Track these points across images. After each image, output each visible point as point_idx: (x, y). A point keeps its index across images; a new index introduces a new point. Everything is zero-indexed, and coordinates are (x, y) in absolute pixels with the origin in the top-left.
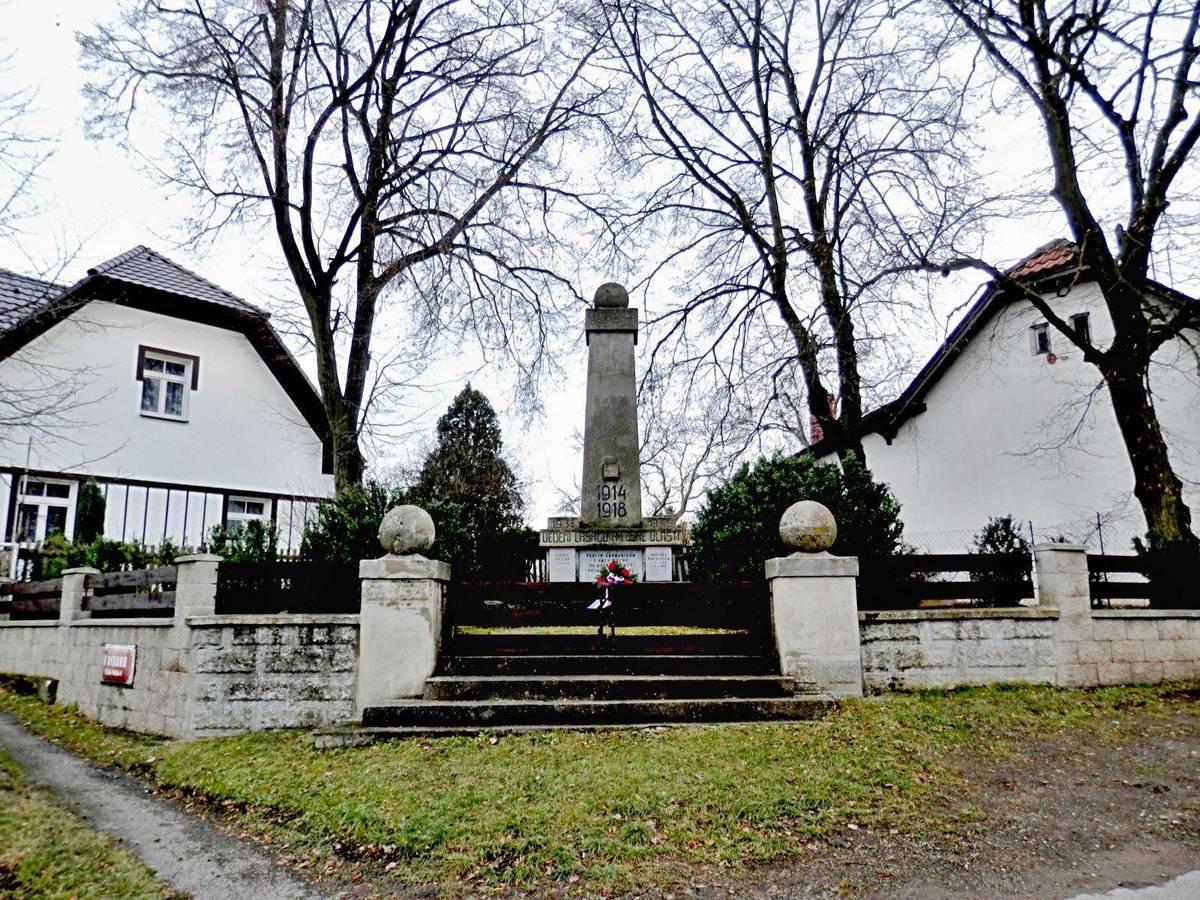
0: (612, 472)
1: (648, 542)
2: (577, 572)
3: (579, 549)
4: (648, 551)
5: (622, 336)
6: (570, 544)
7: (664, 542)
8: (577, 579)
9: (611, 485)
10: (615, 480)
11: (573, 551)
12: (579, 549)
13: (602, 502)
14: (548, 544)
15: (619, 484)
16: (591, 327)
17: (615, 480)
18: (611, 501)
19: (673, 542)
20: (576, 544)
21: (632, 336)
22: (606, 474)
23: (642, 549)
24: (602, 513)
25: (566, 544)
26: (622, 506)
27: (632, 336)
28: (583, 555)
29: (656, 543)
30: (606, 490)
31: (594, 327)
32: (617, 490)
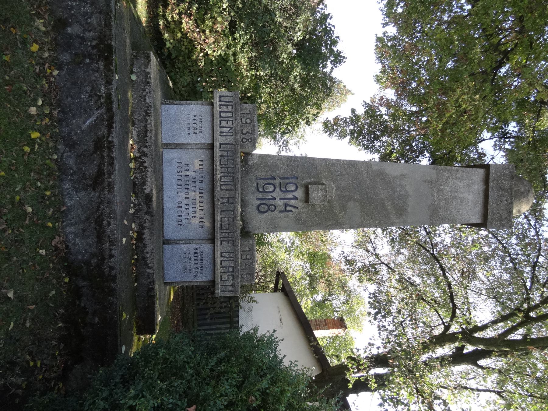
0: (316, 194)
1: (219, 249)
3: (211, 147)
4: (206, 248)
5: (479, 208)
6: (217, 134)
7: (219, 270)
8: (168, 146)
9: (300, 193)
10: (307, 200)
11: (209, 141)
12: (211, 147)
13: (277, 182)
16: (492, 171)
17: (307, 200)
18: (277, 194)
19: (219, 284)
20: (217, 144)
21: (476, 219)
22: (312, 188)
23: (212, 240)
24: (262, 183)
26: (271, 208)
27: (476, 219)
28: (203, 155)
29: (218, 260)
31: (492, 176)
32: (292, 202)
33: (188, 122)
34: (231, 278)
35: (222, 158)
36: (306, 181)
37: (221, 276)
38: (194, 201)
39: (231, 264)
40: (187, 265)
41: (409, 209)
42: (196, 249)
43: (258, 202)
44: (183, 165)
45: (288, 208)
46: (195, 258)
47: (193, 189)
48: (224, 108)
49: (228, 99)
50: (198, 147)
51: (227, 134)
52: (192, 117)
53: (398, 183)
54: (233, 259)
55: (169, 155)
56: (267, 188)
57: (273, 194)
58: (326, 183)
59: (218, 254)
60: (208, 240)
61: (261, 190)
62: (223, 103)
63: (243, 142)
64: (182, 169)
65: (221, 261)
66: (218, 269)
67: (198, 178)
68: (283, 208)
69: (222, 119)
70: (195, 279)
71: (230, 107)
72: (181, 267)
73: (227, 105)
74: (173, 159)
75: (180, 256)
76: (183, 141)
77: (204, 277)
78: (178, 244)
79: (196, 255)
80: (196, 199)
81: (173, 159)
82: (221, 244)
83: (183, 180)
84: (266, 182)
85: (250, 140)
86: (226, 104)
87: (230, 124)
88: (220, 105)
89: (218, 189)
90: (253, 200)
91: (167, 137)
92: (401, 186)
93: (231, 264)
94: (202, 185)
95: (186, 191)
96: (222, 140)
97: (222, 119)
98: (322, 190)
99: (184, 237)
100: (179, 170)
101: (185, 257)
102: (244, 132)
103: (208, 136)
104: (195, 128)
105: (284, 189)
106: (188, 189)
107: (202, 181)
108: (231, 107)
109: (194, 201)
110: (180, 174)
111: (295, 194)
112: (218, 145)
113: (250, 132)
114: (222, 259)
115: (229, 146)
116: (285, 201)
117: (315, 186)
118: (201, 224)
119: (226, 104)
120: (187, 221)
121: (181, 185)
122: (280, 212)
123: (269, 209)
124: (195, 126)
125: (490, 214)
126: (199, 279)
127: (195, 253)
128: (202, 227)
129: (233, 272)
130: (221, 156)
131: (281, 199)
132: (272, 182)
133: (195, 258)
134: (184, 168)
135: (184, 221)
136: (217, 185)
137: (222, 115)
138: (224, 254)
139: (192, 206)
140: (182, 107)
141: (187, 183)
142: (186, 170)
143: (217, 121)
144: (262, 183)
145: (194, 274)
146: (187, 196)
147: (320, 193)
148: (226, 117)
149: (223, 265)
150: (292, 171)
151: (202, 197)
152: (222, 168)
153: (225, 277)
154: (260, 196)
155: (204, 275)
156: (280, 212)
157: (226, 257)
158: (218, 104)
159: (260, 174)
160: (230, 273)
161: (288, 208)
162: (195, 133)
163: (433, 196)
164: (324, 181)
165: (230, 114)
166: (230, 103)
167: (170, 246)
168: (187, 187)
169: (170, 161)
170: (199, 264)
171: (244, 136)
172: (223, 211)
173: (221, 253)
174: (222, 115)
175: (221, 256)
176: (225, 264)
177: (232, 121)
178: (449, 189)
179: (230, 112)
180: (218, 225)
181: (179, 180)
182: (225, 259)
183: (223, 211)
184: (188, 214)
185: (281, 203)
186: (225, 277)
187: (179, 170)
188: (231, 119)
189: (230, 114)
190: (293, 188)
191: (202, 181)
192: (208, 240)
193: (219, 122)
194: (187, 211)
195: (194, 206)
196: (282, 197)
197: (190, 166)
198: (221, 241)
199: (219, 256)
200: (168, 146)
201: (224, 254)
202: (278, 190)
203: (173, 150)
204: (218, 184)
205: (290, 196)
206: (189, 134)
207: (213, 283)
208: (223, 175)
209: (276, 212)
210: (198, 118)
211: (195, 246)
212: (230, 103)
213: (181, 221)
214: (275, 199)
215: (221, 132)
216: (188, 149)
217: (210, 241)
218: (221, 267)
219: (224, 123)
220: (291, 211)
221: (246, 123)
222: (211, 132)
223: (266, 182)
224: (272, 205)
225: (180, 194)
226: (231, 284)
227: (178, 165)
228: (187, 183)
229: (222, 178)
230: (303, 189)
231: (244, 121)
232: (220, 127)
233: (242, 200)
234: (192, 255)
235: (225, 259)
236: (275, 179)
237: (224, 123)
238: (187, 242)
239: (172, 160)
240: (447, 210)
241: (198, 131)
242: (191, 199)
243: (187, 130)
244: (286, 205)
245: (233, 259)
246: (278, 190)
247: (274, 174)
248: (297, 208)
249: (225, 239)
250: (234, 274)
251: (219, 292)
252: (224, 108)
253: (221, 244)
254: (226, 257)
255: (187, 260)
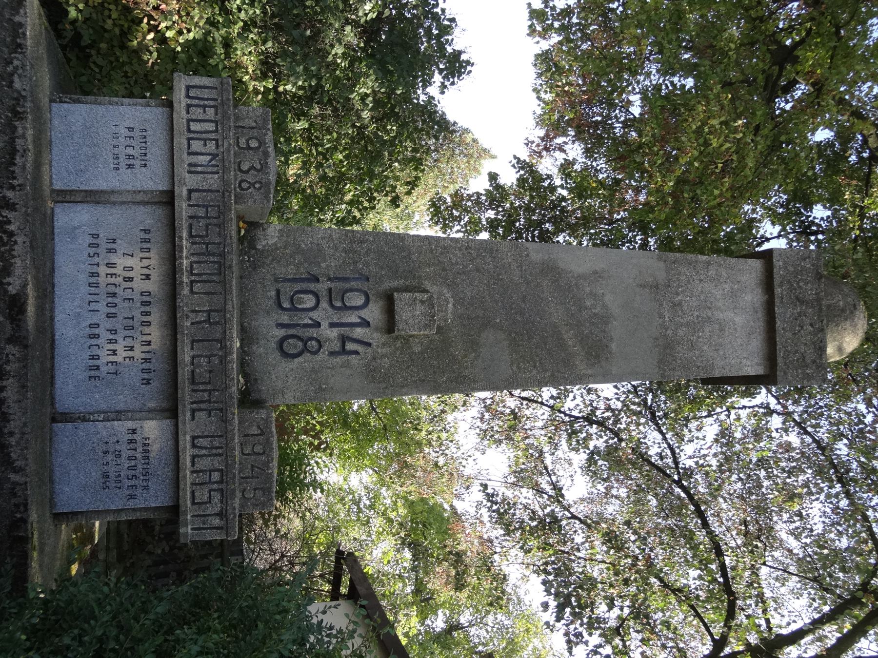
0: (410, 313)
2: (93, 197)
3: (168, 199)
5: (757, 343)
6: (181, 170)
8: (66, 196)
9: (374, 313)
10: (390, 325)
11: (162, 185)
12: (168, 199)
13: (322, 287)
14: (180, 97)
15: (376, 337)
16: (778, 263)
17: (390, 325)
19: (189, 512)
20: (182, 192)
21: (753, 367)
22: (402, 300)
23: (172, 412)
24: (288, 289)
25: (184, 160)
28: (149, 217)
30: (359, 301)
31: (779, 273)
32: (359, 332)
33: (115, 142)
34: (216, 497)
35: (194, 222)
36: (388, 285)
37: (193, 493)
38: (130, 322)
39: (217, 463)
40: (112, 470)
41: (613, 346)
42: (134, 431)
43: (282, 333)
44: (102, 241)
45: (350, 346)
46: (131, 453)
47: (128, 294)
48: (197, 113)
49: (206, 94)
50: (139, 198)
51: (205, 169)
52: (124, 132)
53: (588, 289)
54: (220, 451)
55: (70, 219)
56: (300, 301)
57: (315, 315)
58: (434, 289)
59: (186, 440)
60: (162, 410)
61: (286, 305)
62: (196, 102)
63: (242, 189)
64: (102, 250)
65: (193, 457)
66: (185, 476)
67: (137, 268)
68: (336, 346)
69: (192, 135)
70: (131, 504)
71: (211, 112)
72: (96, 475)
73: (204, 107)
74: (80, 227)
75: (94, 449)
76: (100, 185)
77: (155, 497)
78: (89, 421)
79: (132, 446)
80: (133, 318)
81: (80, 227)
82: (193, 418)
83: (102, 274)
84: (298, 287)
85: (257, 186)
86: (202, 103)
87: (211, 147)
88: (189, 106)
89: (186, 291)
90: (270, 329)
91: (65, 174)
92: (593, 295)
93: (217, 463)
94: (149, 286)
95: (110, 300)
96: (192, 181)
97: (192, 135)
98: (422, 302)
99: (104, 406)
100: (92, 251)
101: (106, 452)
102: (245, 168)
103: (161, 173)
104: (130, 157)
105: (339, 304)
106: (114, 295)
107: (148, 277)
108: (212, 111)
109: (130, 322)
110: (96, 260)
111: (366, 314)
112: (185, 193)
113: (259, 167)
114: (196, 451)
115: (210, 196)
116: (343, 330)
117: (407, 296)
118: (146, 376)
119: (202, 103)
120: (112, 368)
121: (97, 285)
122: (332, 354)
123: (305, 349)
124: (130, 151)
125: (780, 354)
126: (139, 503)
127: (131, 441)
128: (148, 382)
129: (221, 482)
130: (191, 217)
131: (332, 325)
132: (312, 286)
133: (131, 453)
134: (104, 246)
135: (104, 369)
136: (182, 283)
137: (194, 126)
138: (201, 442)
139: (122, 333)
140: (100, 110)
141: (113, 280)
142: (110, 251)
143: (181, 141)
144: (288, 289)
145: (128, 492)
146: (113, 310)
147: (419, 309)
148: (201, 132)
149: (198, 466)
150: (355, 263)
151: (148, 314)
152: (193, 243)
153: (202, 495)
154: (285, 318)
155: (152, 492)
156: (332, 354)
157: (205, 448)
158: (184, 104)
159: (284, 270)
160: (215, 486)
161: (350, 346)
162: (130, 166)
163: (661, 316)
164: (427, 284)
165: (211, 127)
166: (212, 103)
167: (69, 425)
168: (112, 289)
169: (72, 231)
170: (140, 466)
171: (245, 177)
172: (198, 341)
173: (194, 438)
174: (194, 126)
175: (194, 446)
176: (202, 464)
177: (217, 140)
178: (694, 303)
179: (211, 121)
180: (184, 373)
181: (93, 275)
182: (204, 452)
183: (198, 341)
184: (114, 353)
185: (334, 333)
186: (202, 495)
187: (92, 251)
188: (213, 136)
189: (211, 127)
190: (359, 301)
191: (148, 277)
192: (162, 410)
193: (186, 142)
194: (111, 347)
195: (128, 333)
196: (335, 320)
197: (119, 241)
198: (193, 411)
199: (188, 446)
200: (66, 196)
201: (201, 442)
202: (324, 304)
203: (79, 207)
204: (185, 280)
205: (354, 319)
206: (118, 169)
207: (174, 510)
208: (195, 259)
209: (323, 356)
210: (137, 134)
211: (130, 424)
212: (212, 103)
213: (98, 368)
214: (318, 325)
215: (190, 165)
216: (114, 203)
217: (167, 414)
218: (193, 472)
219: (196, 146)
220: (356, 353)
221: (249, 148)
222: (166, 165)
223: (298, 287)
224: (312, 338)
225: (93, 306)
226: (217, 510)
227: (89, 240)
228: (113, 280)
229: (195, 265)
230: (381, 303)
231: (242, 142)
232: (189, 154)
233: (243, 330)
234: (123, 447)
235: (204, 452)
236: (318, 280)
237: (196, 146)
238: (112, 416)
239: (75, 228)
240: (692, 347)
241: (137, 163)
242: (120, 317)
243: (111, 160)
244: (344, 339)
245: (220, 451)
246: (324, 304)
247: (315, 271)
248: (369, 345)
249: (203, 406)
250: (223, 486)
251: (187, 531)
252: (197, 113)
253: (193, 418)
254: (205, 448)
255: (110, 457)
